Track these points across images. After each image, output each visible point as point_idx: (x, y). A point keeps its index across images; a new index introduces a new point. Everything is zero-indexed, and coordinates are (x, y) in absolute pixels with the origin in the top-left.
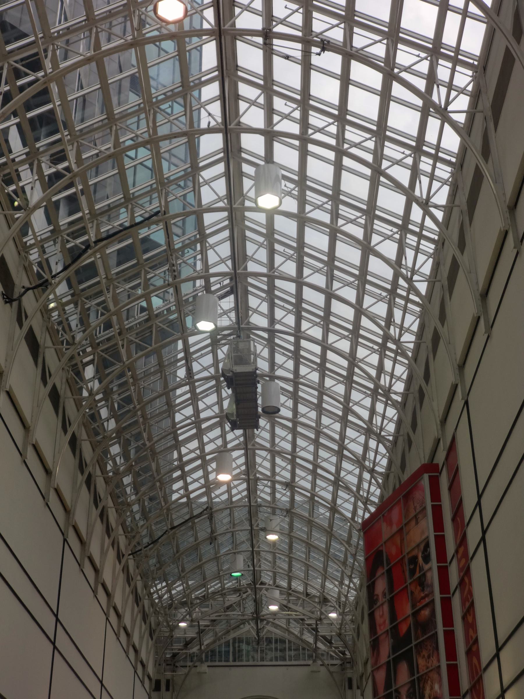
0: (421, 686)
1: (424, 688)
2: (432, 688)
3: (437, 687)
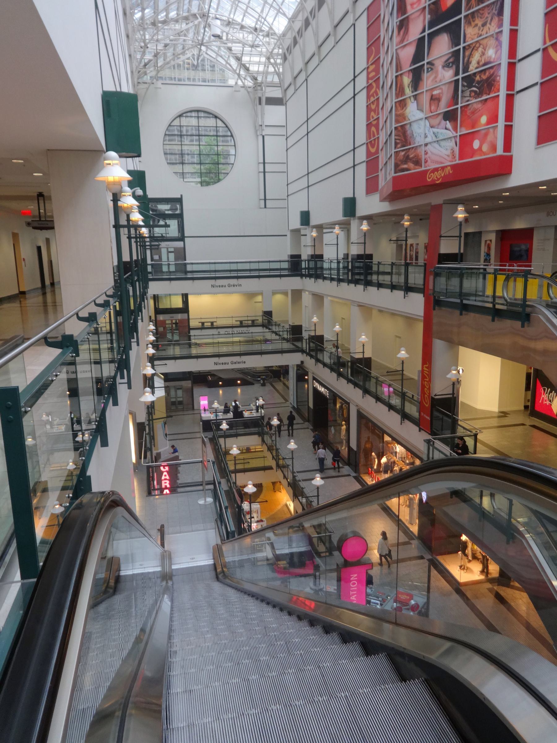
0: (467, 53)
1: (471, 55)
2: (483, 54)
3: (491, 53)
